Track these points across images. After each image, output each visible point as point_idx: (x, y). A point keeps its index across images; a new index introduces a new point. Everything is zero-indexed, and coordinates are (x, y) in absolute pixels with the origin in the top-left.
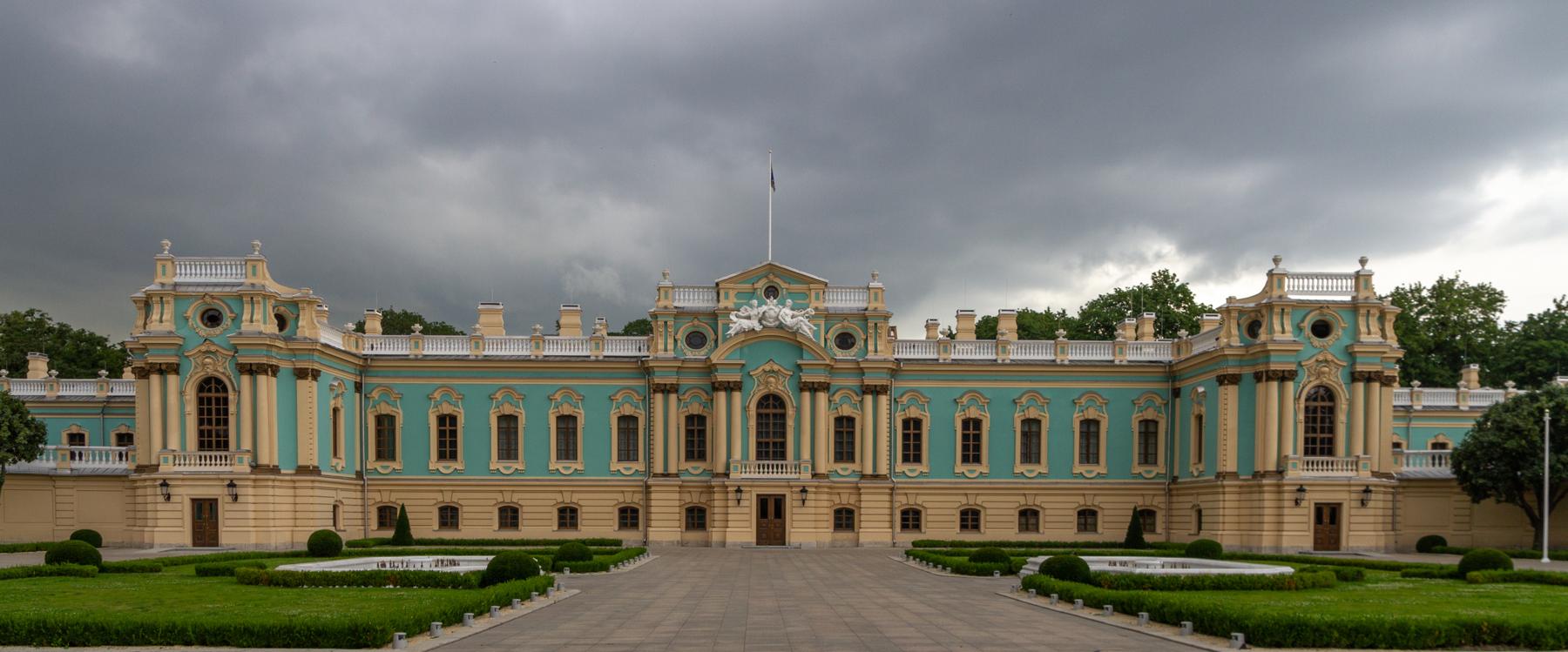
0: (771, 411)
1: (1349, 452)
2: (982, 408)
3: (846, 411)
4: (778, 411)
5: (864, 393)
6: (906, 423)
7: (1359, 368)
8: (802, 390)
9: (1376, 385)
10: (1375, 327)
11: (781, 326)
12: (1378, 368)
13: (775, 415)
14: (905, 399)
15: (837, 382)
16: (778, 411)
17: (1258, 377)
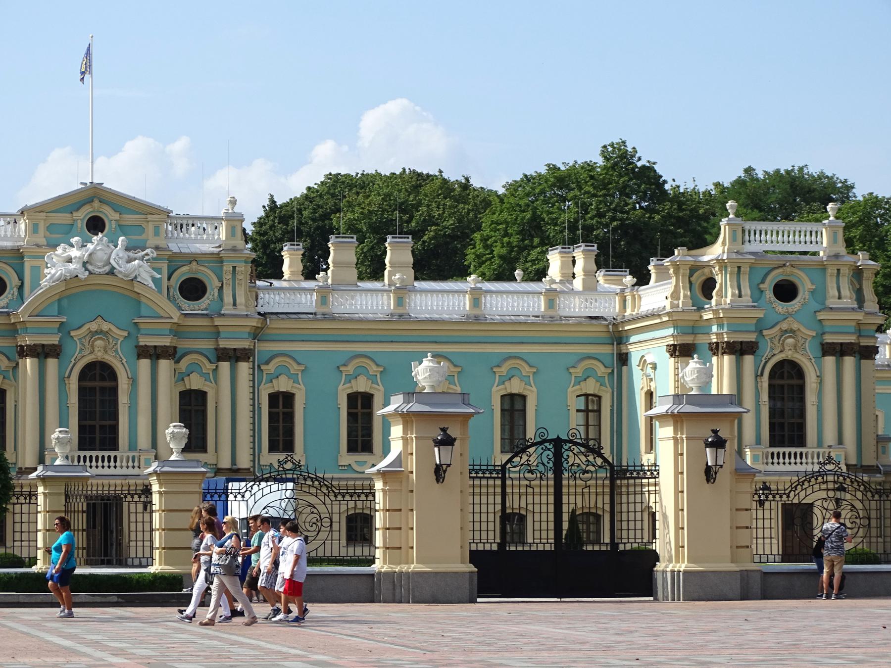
0: (97, 384)
1: (820, 444)
2: (372, 379)
3: (195, 383)
4: (107, 384)
5: (220, 358)
6: (274, 398)
7: (829, 339)
8: (139, 357)
9: (849, 362)
10: (846, 291)
11: (112, 272)
12: (851, 339)
13: (103, 389)
14: (271, 368)
15: (184, 345)
16: (107, 384)
17: (715, 349)
